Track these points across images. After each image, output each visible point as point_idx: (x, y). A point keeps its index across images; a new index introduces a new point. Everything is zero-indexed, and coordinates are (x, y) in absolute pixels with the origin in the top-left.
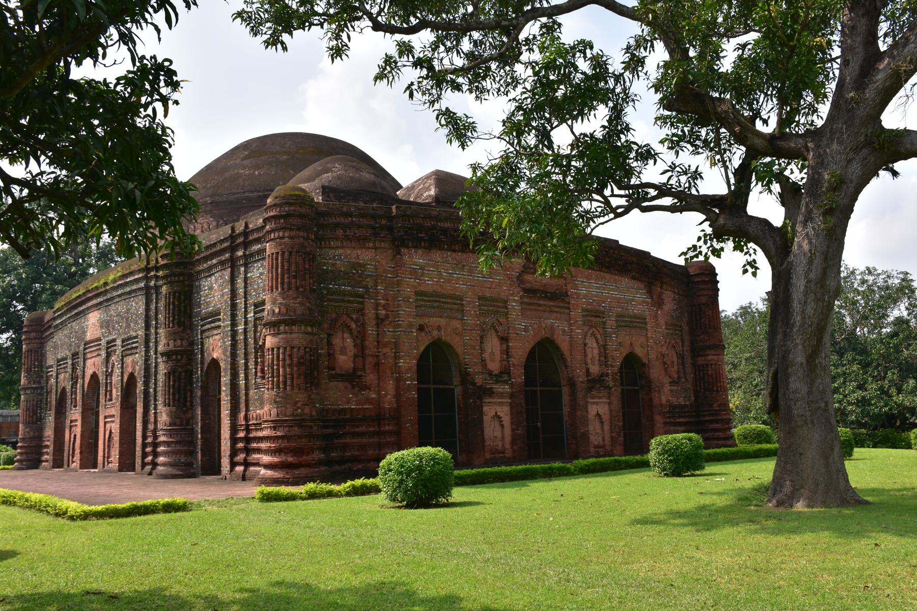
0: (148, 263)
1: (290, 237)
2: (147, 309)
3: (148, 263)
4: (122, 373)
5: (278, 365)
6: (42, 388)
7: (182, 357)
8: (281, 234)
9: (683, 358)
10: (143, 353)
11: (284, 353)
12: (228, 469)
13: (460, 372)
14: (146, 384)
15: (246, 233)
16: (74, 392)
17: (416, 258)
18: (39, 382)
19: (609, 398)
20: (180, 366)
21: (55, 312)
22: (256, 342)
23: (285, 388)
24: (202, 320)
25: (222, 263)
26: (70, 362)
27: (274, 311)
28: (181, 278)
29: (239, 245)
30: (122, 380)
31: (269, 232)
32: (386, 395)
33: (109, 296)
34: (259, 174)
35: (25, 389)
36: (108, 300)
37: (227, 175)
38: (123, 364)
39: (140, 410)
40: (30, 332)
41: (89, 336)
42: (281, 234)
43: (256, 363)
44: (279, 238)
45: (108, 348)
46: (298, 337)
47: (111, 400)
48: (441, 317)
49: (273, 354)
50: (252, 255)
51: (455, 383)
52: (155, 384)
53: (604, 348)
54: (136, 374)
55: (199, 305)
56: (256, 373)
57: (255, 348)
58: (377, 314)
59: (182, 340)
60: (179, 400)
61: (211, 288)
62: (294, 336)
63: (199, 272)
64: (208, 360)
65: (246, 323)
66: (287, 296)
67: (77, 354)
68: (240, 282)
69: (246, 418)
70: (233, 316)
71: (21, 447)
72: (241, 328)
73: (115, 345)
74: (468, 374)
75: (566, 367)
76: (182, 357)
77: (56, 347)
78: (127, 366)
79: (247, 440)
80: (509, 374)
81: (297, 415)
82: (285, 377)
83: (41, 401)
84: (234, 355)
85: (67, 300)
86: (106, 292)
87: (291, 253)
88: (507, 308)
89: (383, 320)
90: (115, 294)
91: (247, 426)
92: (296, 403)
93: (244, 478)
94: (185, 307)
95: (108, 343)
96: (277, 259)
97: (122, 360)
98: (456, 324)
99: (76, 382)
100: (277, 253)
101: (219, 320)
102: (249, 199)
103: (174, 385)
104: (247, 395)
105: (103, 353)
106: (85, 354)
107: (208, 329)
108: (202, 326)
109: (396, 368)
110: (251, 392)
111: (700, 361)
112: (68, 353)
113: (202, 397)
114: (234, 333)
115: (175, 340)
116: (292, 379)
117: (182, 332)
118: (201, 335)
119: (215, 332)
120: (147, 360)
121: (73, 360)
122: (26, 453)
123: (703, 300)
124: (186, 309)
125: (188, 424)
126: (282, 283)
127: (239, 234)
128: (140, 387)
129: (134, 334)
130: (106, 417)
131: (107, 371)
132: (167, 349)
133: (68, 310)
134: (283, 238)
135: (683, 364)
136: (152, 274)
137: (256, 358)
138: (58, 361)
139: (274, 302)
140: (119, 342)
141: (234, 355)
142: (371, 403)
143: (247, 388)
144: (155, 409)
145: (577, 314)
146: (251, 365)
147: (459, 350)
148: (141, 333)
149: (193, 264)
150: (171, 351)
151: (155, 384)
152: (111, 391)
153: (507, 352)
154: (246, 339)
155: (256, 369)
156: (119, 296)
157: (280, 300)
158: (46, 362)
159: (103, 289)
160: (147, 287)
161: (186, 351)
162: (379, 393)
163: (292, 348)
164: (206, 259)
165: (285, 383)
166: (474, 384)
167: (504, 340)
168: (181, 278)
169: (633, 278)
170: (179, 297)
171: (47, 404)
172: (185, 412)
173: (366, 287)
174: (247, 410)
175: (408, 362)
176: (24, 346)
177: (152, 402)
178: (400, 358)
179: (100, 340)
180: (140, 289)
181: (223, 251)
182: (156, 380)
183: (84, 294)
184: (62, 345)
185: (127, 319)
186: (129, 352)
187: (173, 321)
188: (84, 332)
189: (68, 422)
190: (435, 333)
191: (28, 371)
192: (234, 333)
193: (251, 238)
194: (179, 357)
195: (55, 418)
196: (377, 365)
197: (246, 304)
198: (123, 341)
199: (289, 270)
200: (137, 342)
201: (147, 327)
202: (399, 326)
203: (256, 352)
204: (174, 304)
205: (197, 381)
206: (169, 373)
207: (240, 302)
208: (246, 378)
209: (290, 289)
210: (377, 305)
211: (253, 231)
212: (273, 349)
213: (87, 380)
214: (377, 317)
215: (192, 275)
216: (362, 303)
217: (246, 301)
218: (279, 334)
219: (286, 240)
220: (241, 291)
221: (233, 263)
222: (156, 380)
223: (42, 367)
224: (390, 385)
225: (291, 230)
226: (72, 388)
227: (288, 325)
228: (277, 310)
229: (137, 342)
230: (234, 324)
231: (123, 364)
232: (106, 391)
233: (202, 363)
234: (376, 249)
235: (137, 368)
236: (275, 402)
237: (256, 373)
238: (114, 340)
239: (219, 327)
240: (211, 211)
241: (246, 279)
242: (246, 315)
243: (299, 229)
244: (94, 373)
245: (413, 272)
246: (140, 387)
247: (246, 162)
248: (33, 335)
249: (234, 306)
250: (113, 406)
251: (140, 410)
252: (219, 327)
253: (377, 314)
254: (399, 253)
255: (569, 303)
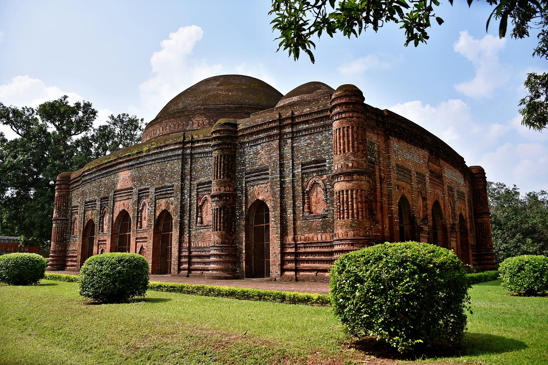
0: (184, 139)
1: (357, 117)
2: (183, 168)
3: (184, 139)
4: (155, 210)
5: (352, 201)
6: (68, 220)
7: (230, 198)
8: (351, 115)
9: (472, 219)
10: (180, 197)
11: (356, 194)
12: (279, 273)
13: (410, 217)
14: (182, 217)
15: (293, 117)
16: (101, 221)
17: (395, 144)
18: (66, 216)
19: (456, 238)
20: (229, 204)
21: (84, 172)
22: (303, 189)
23: (358, 218)
24: (246, 174)
25: (270, 137)
26: (98, 203)
27: (347, 165)
28: (229, 146)
29: (287, 125)
30: (155, 214)
31: (339, 113)
32: (386, 227)
33: (141, 160)
34: (232, 95)
35: (56, 220)
36: (140, 163)
37: (210, 93)
38: (155, 204)
39: (175, 234)
40: (61, 185)
41: (119, 187)
42: (351, 115)
43: (304, 203)
44: (349, 117)
45: (139, 194)
46: (364, 183)
47: (141, 228)
48: (403, 181)
49: (347, 194)
50: (299, 132)
51: (404, 224)
52: (190, 217)
53: (453, 209)
54: (171, 210)
55: (244, 164)
56: (303, 209)
57: (303, 193)
58: (380, 176)
59: (229, 187)
60: (227, 227)
61: (257, 153)
62: (363, 182)
63: (244, 143)
64: (251, 201)
65: (293, 176)
66: (357, 156)
67: (107, 198)
68: (287, 150)
69: (294, 239)
70: (281, 172)
71: (52, 256)
72: (288, 179)
73: (148, 192)
74: (414, 218)
75: (442, 218)
76: (230, 198)
77: (83, 194)
78: (161, 205)
79: (296, 254)
80: (427, 219)
81: (366, 236)
82: (357, 209)
83: (66, 228)
84: (282, 197)
85: (96, 165)
86: (139, 158)
87: (358, 127)
88: (425, 180)
89: (383, 179)
90: (147, 159)
91: (296, 244)
92: (365, 228)
93: (297, 280)
94: (232, 165)
95: (139, 191)
96: (348, 131)
97: (155, 201)
98: (409, 187)
99: (103, 217)
100: (348, 127)
101: (268, 174)
102: (230, 108)
103: (223, 217)
104: (294, 224)
105: (135, 198)
106: (114, 198)
107: (253, 181)
108: (246, 178)
109: (391, 212)
110: (298, 223)
111: (479, 220)
112: (96, 197)
113: (246, 226)
114: (282, 183)
115: (225, 187)
116: (362, 211)
117: (230, 182)
118: (245, 184)
119: (261, 182)
120: (182, 200)
121: (101, 202)
122: (56, 260)
123: (481, 187)
124: (232, 167)
125: (233, 243)
126: (353, 147)
127: (287, 119)
128: (175, 218)
129: (169, 184)
130: (137, 239)
131: (138, 209)
132: (218, 192)
133: (97, 171)
134: (352, 117)
135: (472, 222)
136: (188, 145)
137: (304, 199)
138: (86, 203)
139: (347, 159)
140: (152, 190)
141: (282, 197)
142: (380, 233)
143: (295, 220)
144: (190, 232)
145: (446, 187)
146: (299, 203)
147: (410, 203)
148: (177, 184)
149: (237, 138)
150: (223, 194)
151: (190, 217)
152: (141, 222)
153: (425, 206)
154: (293, 187)
155: (303, 206)
156: (152, 160)
157: (352, 158)
158: (71, 204)
159: (135, 157)
160: (183, 154)
161: (232, 195)
162: (383, 227)
163: (362, 190)
164: (251, 134)
165: (358, 213)
166: (417, 224)
167: (424, 199)
168: (229, 146)
169: (460, 171)
170: (228, 159)
171: (71, 230)
172: (231, 235)
173: (375, 157)
174: (295, 234)
175: (395, 208)
176: (56, 193)
177: (187, 229)
178: (392, 204)
179: (132, 189)
180: (178, 155)
181: (273, 128)
182: (190, 214)
183: (115, 160)
184: (90, 193)
185: (161, 176)
186: (164, 196)
187: (223, 174)
188: (115, 184)
189: (96, 242)
190: (402, 190)
191: (59, 209)
192: (282, 183)
193: (284, 123)
194: (228, 198)
195: (83, 239)
196: (382, 207)
197: (293, 164)
198: (156, 189)
199: (357, 138)
200: (171, 190)
201: (183, 180)
202: (391, 184)
203: (303, 196)
204: (224, 163)
205: (241, 214)
206: (220, 209)
207: (288, 163)
208: (294, 213)
209: (358, 151)
210: (380, 170)
211: (299, 116)
212: (347, 191)
213: (116, 215)
214: (380, 178)
215: (236, 145)
216: (373, 167)
217: (293, 162)
218: (352, 181)
219: (355, 118)
220: (289, 156)
221: (281, 136)
222: (190, 214)
223: (68, 206)
224: (387, 221)
225: (358, 112)
226: (100, 219)
227: (359, 175)
228: (350, 165)
229: (171, 190)
230: (282, 176)
231: (155, 204)
232: (137, 222)
233: (246, 203)
234: (378, 134)
235: (172, 207)
236: (351, 226)
237: (303, 209)
238: (148, 189)
239: (268, 178)
240: (204, 114)
241: (292, 148)
242: (293, 171)
243: (362, 113)
244: (124, 210)
245: (395, 152)
246: (175, 218)
247: (221, 87)
248: (63, 186)
249: (282, 165)
250: (145, 231)
251: (175, 234)
252: (268, 178)
253: (380, 176)
254: (389, 139)
255: (443, 181)
